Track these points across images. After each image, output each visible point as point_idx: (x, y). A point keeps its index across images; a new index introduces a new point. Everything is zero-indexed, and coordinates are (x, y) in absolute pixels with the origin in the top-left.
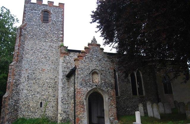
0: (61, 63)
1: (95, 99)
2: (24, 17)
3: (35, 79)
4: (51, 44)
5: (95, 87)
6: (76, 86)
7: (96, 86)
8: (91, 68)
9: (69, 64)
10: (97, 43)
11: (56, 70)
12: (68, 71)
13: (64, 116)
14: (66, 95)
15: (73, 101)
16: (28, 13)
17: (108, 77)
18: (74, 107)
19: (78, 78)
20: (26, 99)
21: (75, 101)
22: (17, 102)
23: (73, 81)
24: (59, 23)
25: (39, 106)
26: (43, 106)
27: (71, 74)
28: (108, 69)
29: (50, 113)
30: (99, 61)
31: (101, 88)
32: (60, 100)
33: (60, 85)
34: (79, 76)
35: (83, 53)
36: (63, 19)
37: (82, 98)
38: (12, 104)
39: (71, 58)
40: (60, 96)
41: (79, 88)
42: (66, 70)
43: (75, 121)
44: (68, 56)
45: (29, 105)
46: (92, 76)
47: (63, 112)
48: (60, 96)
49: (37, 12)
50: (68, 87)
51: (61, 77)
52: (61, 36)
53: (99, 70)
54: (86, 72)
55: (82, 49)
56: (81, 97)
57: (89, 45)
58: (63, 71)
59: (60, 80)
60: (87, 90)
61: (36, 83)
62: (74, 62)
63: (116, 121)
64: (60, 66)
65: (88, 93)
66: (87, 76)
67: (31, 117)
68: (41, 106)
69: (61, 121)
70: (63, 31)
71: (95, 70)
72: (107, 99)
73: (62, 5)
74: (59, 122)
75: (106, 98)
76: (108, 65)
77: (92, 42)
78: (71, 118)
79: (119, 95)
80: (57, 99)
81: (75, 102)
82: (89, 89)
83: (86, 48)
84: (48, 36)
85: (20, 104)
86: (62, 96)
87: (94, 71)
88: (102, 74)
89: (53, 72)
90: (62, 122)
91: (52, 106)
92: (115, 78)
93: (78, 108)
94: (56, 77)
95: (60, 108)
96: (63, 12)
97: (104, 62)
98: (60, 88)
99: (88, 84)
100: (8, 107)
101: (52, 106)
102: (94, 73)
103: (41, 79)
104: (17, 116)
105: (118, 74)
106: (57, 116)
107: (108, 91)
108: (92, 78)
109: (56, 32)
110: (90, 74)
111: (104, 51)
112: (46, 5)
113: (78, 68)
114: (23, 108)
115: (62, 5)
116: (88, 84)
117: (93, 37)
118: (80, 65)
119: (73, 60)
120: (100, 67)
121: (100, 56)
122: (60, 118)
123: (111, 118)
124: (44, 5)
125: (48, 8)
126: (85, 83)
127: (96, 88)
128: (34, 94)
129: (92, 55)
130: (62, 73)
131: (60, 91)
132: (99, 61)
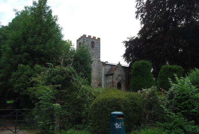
33: (103, 79)
36: (100, 46)
51: (103, 75)
73: (99, 39)
75: (122, 85)
76: (123, 73)
96: (100, 42)
102: (119, 75)
115: (99, 39)
125: (93, 40)
126: (117, 79)
131: (103, 81)
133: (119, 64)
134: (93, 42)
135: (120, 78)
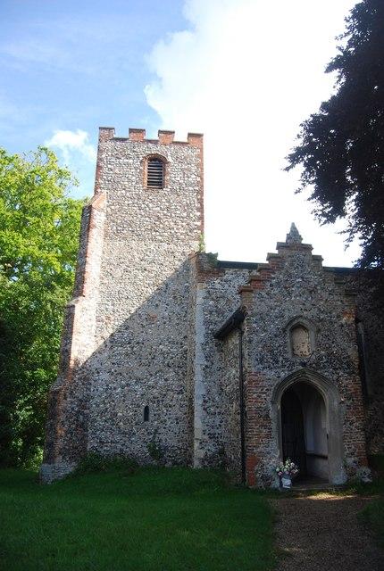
0: (199, 300)
1: (298, 401)
2: (98, 176)
3: (129, 343)
4: (172, 246)
5: (301, 368)
6: (246, 365)
7: (304, 364)
8: (287, 314)
9: (222, 302)
10: (303, 242)
11: (185, 317)
12: (220, 322)
13: (212, 448)
14: (214, 390)
15: (235, 406)
16: (109, 166)
17: (339, 340)
18: (243, 423)
19: (250, 342)
20: (106, 398)
21: (243, 406)
22: (83, 403)
23: (237, 352)
24: (191, 188)
25: (142, 417)
26: (151, 417)
27: (229, 329)
28: (338, 317)
29: (169, 438)
30: (311, 292)
31: (319, 372)
32: (198, 403)
33: (199, 362)
34: (257, 332)
35: (264, 272)
37: (265, 402)
38: (73, 409)
39: (226, 285)
40: (199, 391)
41: (254, 370)
42: (215, 318)
43: (243, 464)
44: (218, 281)
45: (116, 414)
46: (291, 337)
47: (206, 437)
48: (199, 391)
49: (131, 161)
50: (223, 366)
51: (199, 338)
52: (195, 223)
53: (310, 321)
54: (272, 326)
55: (263, 260)
56: (260, 397)
57: (280, 246)
58: (207, 323)
59: (198, 348)
60: (278, 377)
61: (133, 353)
62: (238, 296)
63: (368, 471)
64: (198, 309)
65: (280, 386)
66: (276, 336)
67: (119, 446)
68: (146, 418)
69: (203, 461)
70: (201, 209)
71: (300, 320)
72: (336, 403)
74: (196, 464)
75: (333, 401)
77: (289, 237)
78: (233, 455)
79: (370, 392)
80: (191, 400)
81: (243, 410)
82: (283, 375)
83: (270, 257)
84: (161, 226)
85: (92, 409)
86: (204, 392)
87: (296, 322)
88: (319, 331)
89: (178, 324)
90: (206, 463)
91: (177, 419)
92: (359, 343)
93: (254, 428)
94: (186, 337)
95: (198, 424)
96: (200, 156)
97: (325, 295)
98: (198, 369)
99: (281, 359)
100: (62, 418)
101: (177, 419)
102: (295, 326)
103: (146, 343)
104: (84, 440)
105: (365, 331)
106: (191, 446)
107: (337, 380)
108: (292, 343)
109: (185, 214)
110: (284, 330)
111: (325, 264)
112: (155, 142)
113: (249, 313)
114: (100, 422)
116: (281, 359)
117: (290, 226)
118: (257, 305)
119: (234, 291)
120: (314, 311)
121: (314, 280)
122: (198, 453)
123: (350, 461)
124: (150, 141)
126: (271, 357)
127: (304, 373)
128: (128, 385)
129: (290, 276)
130: (204, 327)
131: (198, 378)
132: (311, 292)
133: (294, 249)
134: (157, 163)
135: (305, 344)
